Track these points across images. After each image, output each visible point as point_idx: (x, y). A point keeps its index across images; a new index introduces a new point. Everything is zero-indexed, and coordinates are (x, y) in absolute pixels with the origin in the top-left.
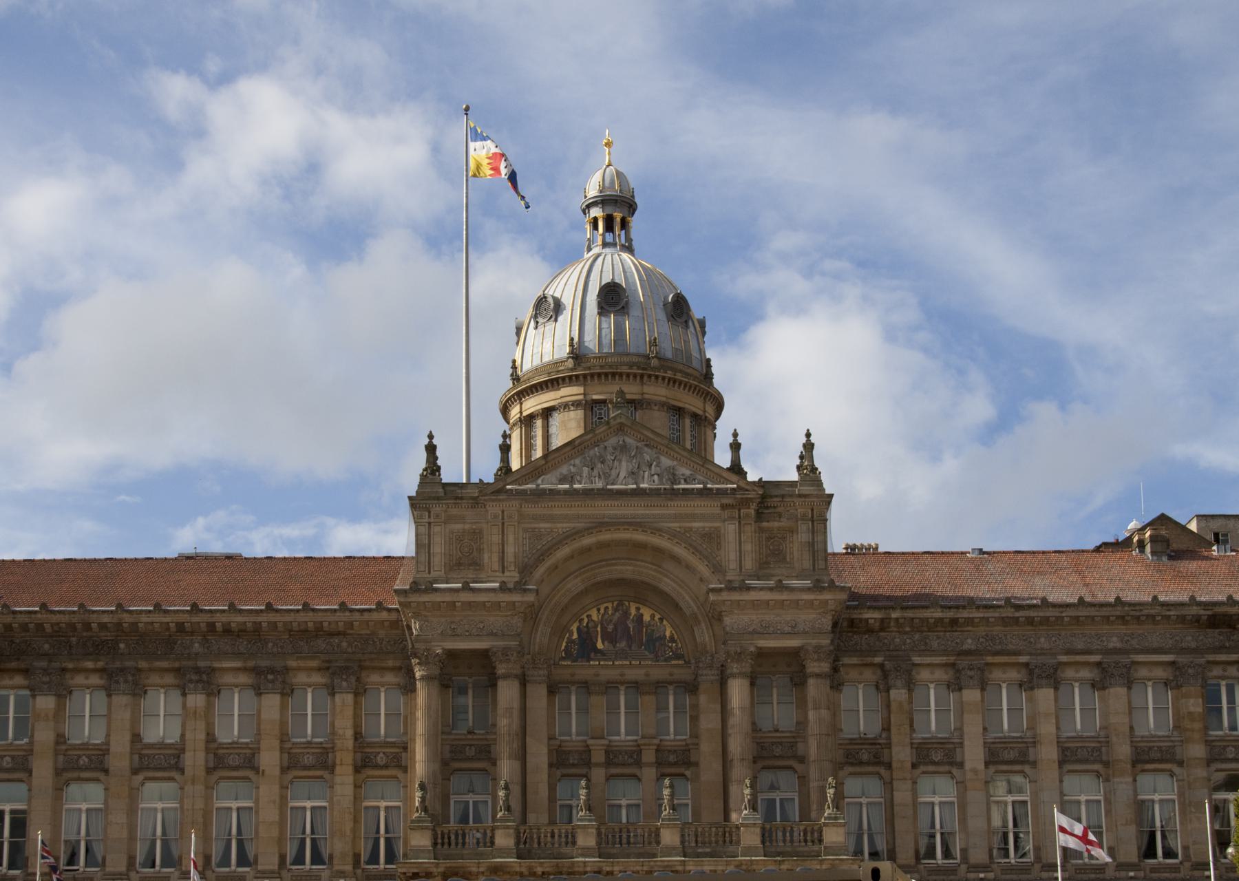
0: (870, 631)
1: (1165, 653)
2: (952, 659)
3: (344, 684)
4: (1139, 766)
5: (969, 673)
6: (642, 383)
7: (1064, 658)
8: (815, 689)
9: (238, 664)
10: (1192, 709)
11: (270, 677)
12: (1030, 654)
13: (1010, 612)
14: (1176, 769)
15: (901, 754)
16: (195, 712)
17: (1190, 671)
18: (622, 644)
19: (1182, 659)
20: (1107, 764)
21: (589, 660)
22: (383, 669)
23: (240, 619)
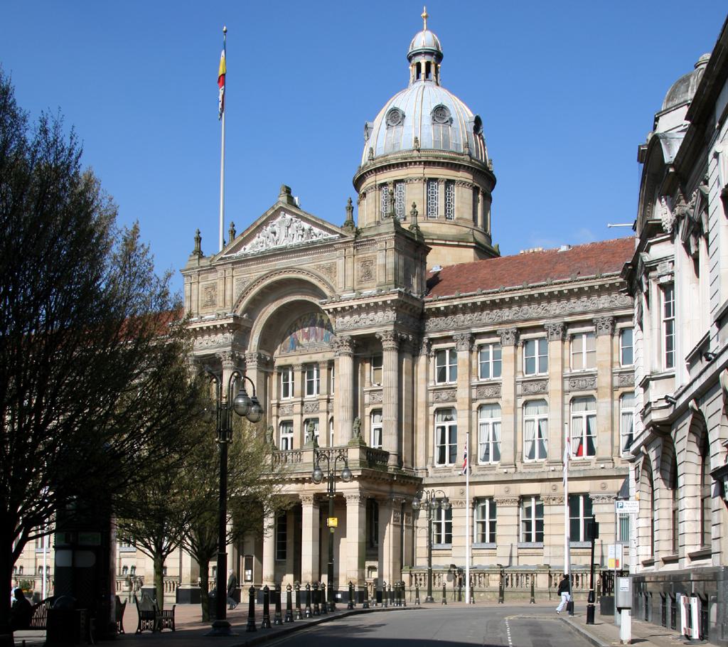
5: (507, 336)
8: (389, 358)
18: (312, 340)
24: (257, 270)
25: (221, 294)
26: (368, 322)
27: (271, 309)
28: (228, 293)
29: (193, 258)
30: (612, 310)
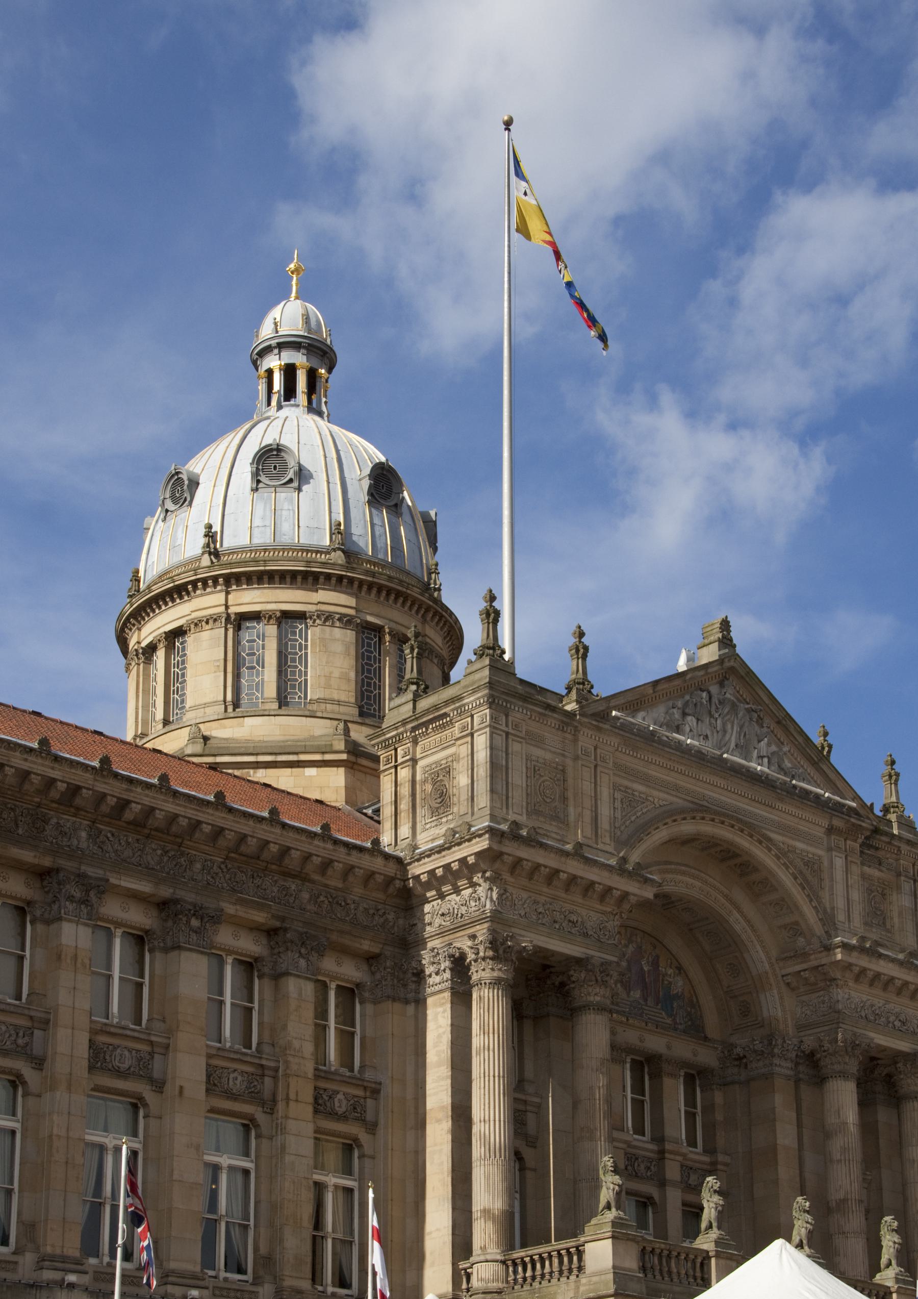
3: (302, 963)
6: (424, 620)
9: (144, 887)
11: (195, 923)
16: (75, 957)
22: (344, 951)
23: (170, 807)
28: (605, 811)
29: (478, 665)
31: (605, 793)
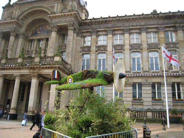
0: (89, 25)
1: (155, 25)
2: (106, 29)
4: (149, 50)
7: (131, 27)
10: (162, 36)
12: (123, 27)
13: (118, 18)
14: (158, 50)
15: (93, 49)
17: (161, 28)
18: (42, 32)
19: (159, 26)
20: (141, 49)
21: (36, 35)
24: (27, 7)
25: (14, 14)
26: (64, 21)
27: (30, 20)
30: (146, 25)
31: (17, 12)
